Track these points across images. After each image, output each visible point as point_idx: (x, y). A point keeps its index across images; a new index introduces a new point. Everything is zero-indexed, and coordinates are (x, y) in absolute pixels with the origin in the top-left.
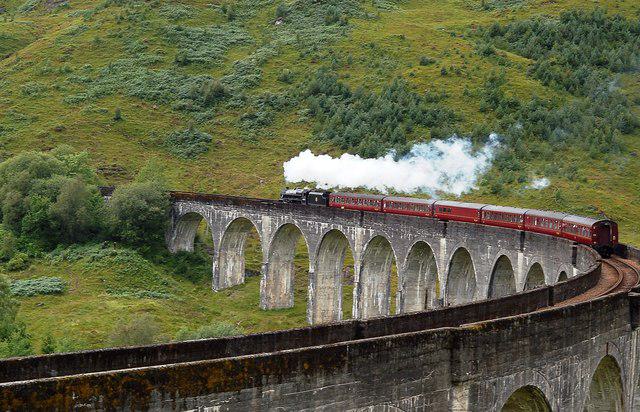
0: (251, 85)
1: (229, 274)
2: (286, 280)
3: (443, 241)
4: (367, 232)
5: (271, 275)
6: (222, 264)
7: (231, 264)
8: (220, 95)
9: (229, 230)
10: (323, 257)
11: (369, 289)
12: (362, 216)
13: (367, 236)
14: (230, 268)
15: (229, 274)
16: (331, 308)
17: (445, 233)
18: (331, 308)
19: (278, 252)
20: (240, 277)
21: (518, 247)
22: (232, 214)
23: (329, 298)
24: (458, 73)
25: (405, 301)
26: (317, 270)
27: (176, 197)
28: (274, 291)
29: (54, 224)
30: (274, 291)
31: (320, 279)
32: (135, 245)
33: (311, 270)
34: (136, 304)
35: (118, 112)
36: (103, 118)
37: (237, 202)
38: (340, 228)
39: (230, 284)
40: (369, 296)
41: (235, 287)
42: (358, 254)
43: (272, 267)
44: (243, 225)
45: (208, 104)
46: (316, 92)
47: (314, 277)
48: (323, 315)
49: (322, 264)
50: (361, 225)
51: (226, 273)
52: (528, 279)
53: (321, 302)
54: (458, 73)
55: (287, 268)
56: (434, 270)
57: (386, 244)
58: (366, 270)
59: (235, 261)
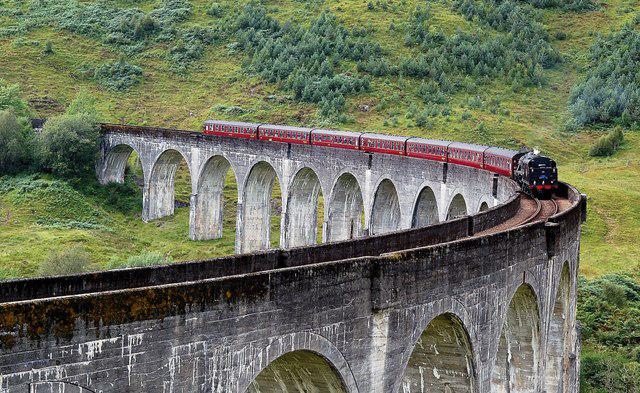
0: (182, 19)
2: (215, 209)
3: (368, 173)
5: (200, 206)
6: (152, 195)
8: (150, 28)
9: (159, 161)
10: (251, 188)
12: (290, 148)
14: (159, 199)
15: (159, 205)
16: (259, 238)
17: (370, 165)
18: (259, 238)
19: (208, 182)
20: (169, 208)
21: (441, 178)
22: (163, 145)
24: (385, 8)
26: (245, 201)
27: (106, 130)
28: (203, 222)
31: (248, 211)
32: (66, 177)
33: (240, 201)
34: (68, 235)
35: (49, 45)
36: (34, 51)
37: (166, 134)
38: (268, 160)
39: (160, 216)
41: (165, 218)
42: (286, 186)
43: (201, 198)
44: (173, 157)
45: (139, 36)
46: (245, 26)
47: (243, 208)
49: (249, 196)
50: (288, 157)
52: (450, 210)
53: (249, 233)
54: (385, 8)
55: (216, 199)
56: (360, 201)
57: (313, 176)
58: (293, 200)
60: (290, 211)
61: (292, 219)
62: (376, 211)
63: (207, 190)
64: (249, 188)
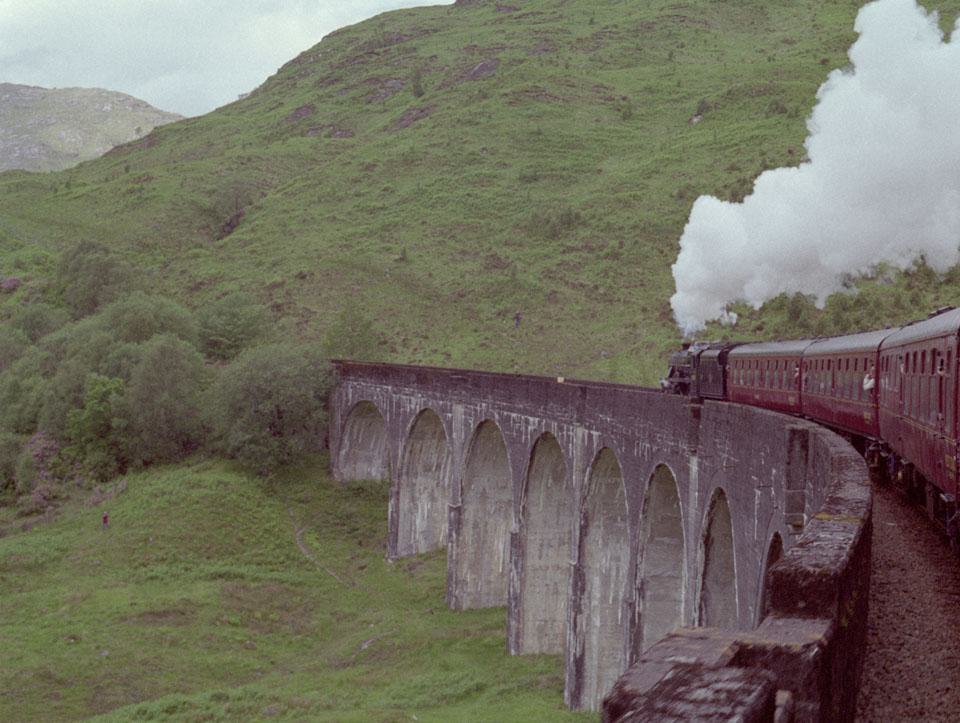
1: (420, 523)
4: (590, 436)
6: (405, 504)
7: (424, 505)
10: (538, 497)
11: (606, 582)
13: (588, 450)
15: (420, 523)
17: (694, 438)
22: (414, 401)
23: (556, 592)
25: (646, 631)
28: (475, 566)
29: (115, 422)
30: (475, 566)
40: (604, 599)
48: (541, 631)
49: (537, 512)
50: (581, 421)
51: (412, 523)
58: (596, 534)
59: (433, 499)
60: (588, 561)
61: (595, 582)
62: (709, 583)
63: (484, 496)
64: (533, 495)
